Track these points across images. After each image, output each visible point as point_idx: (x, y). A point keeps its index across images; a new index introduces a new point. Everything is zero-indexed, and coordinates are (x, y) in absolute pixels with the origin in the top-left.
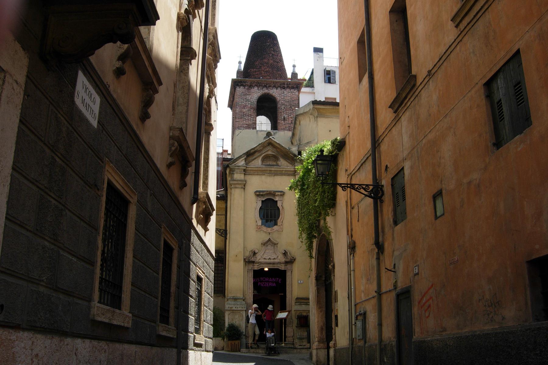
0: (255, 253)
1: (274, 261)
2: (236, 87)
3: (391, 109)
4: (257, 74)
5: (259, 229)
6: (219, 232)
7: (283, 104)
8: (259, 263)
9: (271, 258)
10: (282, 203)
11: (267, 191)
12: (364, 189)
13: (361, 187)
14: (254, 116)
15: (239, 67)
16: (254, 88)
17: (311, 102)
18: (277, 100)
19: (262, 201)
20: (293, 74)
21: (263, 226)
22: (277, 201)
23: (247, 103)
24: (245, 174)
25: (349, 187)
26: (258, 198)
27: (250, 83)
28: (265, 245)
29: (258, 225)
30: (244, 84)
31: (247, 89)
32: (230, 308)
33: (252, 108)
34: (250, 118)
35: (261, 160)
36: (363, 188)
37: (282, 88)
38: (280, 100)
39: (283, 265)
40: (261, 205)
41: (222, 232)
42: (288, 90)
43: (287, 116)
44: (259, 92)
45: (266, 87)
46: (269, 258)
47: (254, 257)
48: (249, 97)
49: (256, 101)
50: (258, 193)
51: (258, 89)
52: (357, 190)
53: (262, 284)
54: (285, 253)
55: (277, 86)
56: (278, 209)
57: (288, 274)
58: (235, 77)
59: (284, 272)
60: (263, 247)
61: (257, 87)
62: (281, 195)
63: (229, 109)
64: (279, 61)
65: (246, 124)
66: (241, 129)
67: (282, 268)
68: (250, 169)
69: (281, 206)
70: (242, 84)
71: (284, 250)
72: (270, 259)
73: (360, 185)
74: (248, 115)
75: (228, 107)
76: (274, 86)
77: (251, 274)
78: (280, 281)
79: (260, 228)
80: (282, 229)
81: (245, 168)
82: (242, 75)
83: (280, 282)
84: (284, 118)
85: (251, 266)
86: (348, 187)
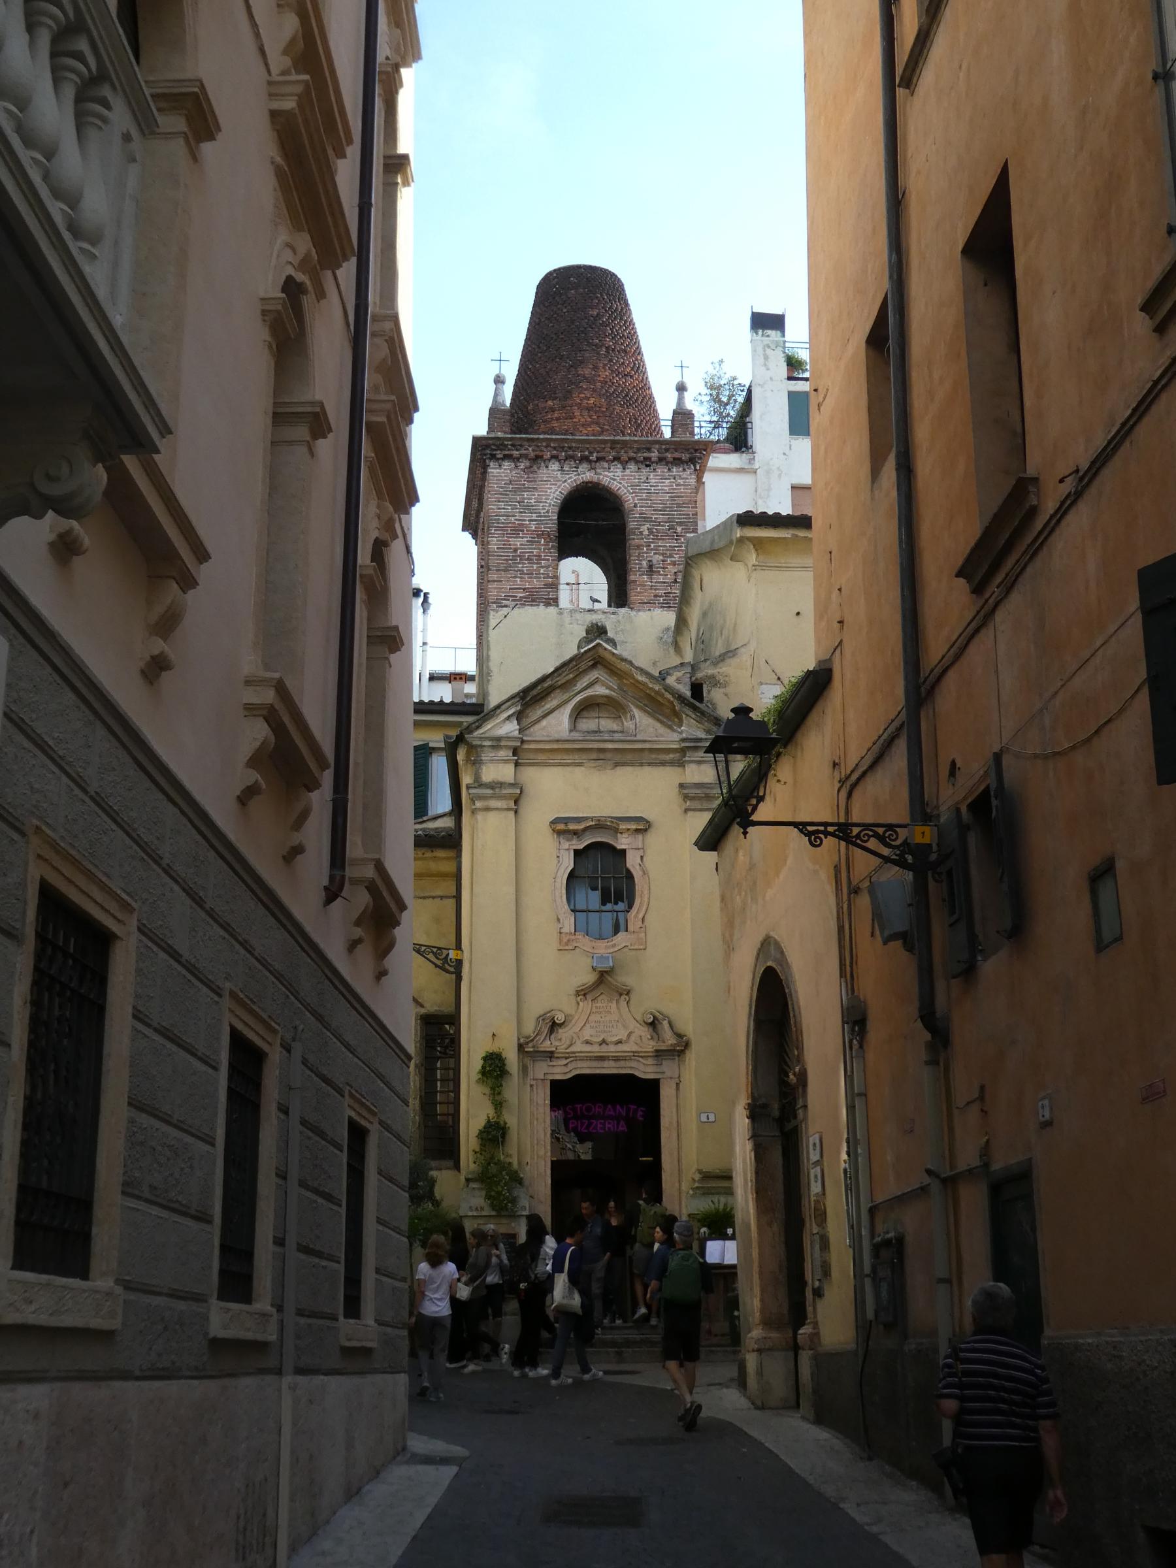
0: (554, 1026)
1: (620, 1047)
2: (487, 461)
3: (962, 581)
4: (558, 419)
5: (567, 944)
6: (437, 958)
7: (647, 519)
8: (566, 1058)
9: (609, 1039)
10: (642, 857)
11: (592, 819)
12: (882, 839)
13: (871, 833)
14: (548, 560)
15: (496, 395)
16: (547, 467)
17: (735, 518)
18: (626, 507)
19: (577, 853)
20: (679, 413)
21: (579, 936)
22: (623, 852)
23: (527, 516)
24: (517, 764)
25: (833, 834)
26: (562, 841)
27: (533, 450)
28: (587, 996)
30: (516, 453)
31: (524, 470)
33: (543, 534)
34: (535, 566)
36: (876, 835)
37: (642, 462)
38: (635, 506)
39: (650, 1061)
40: (571, 866)
42: (661, 470)
43: (661, 558)
44: (566, 481)
45: (590, 462)
46: (601, 1039)
47: (552, 1037)
48: (530, 498)
49: (557, 509)
50: (561, 827)
51: (562, 469)
52: (858, 841)
53: (582, 1124)
54: (653, 1021)
55: (624, 457)
56: (630, 876)
58: (482, 430)
59: (653, 1086)
60: (581, 1004)
61: (557, 464)
62: (637, 831)
63: (467, 536)
64: (632, 369)
65: (524, 589)
66: (506, 606)
67: (645, 1070)
68: (532, 746)
69: (638, 867)
70: (507, 453)
73: (866, 826)
74: (528, 559)
75: (463, 530)
76: (616, 459)
78: (640, 1113)
79: (568, 941)
81: (518, 744)
82: (508, 424)
83: (641, 1119)
84: (651, 567)
86: (827, 834)
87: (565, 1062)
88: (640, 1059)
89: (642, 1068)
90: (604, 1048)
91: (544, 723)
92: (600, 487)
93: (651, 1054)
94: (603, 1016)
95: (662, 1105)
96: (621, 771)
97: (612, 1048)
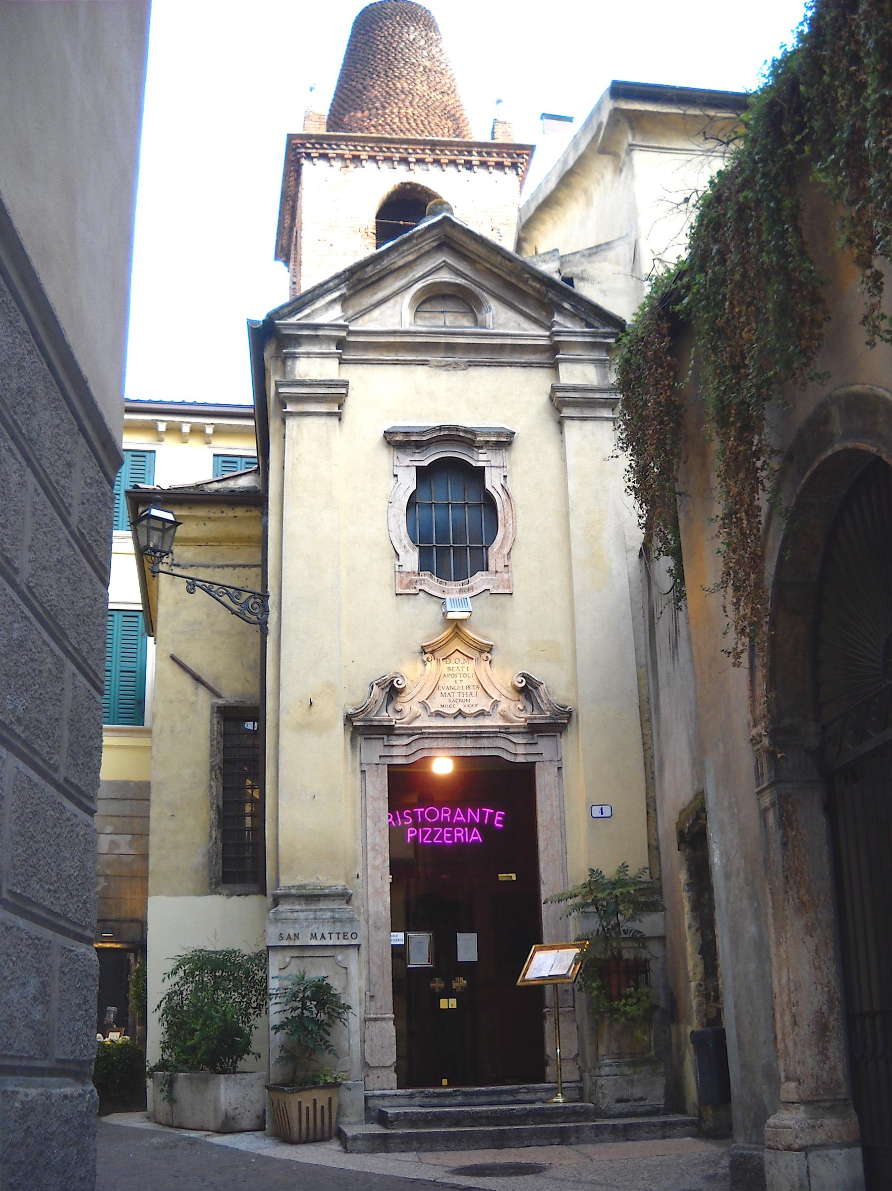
9: (466, 710)
10: (505, 477)
21: (425, 576)
22: (480, 472)
26: (401, 456)
29: (403, 569)
32: (289, 937)
35: (410, 306)
40: (414, 487)
41: (246, 602)
46: (454, 711)
47: (390, 708)
56: (489, 503)
57: (544, 779)
69: (500, 490)
71: (523, 675)
72: (460, 713)
77: (379, 785)
79: (411, 582)
80: (509, 583)
81: (344, 334)
85: (374, 750)
87: (407, 741)
88: (510, 737)
89: (511, 748)
90: (460, 722)
91: (376, 313)
92: (419, 189)
93: (522, 730)
94: (458, 679)
95: (540, 797)
96: (474, 372)
97: (470, 722)
